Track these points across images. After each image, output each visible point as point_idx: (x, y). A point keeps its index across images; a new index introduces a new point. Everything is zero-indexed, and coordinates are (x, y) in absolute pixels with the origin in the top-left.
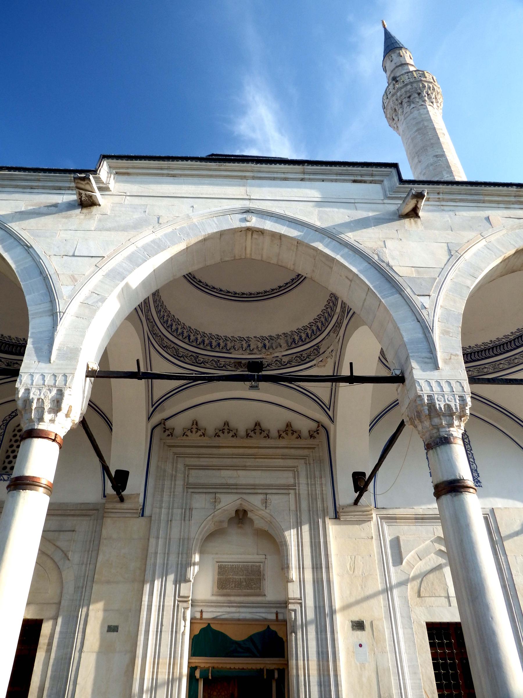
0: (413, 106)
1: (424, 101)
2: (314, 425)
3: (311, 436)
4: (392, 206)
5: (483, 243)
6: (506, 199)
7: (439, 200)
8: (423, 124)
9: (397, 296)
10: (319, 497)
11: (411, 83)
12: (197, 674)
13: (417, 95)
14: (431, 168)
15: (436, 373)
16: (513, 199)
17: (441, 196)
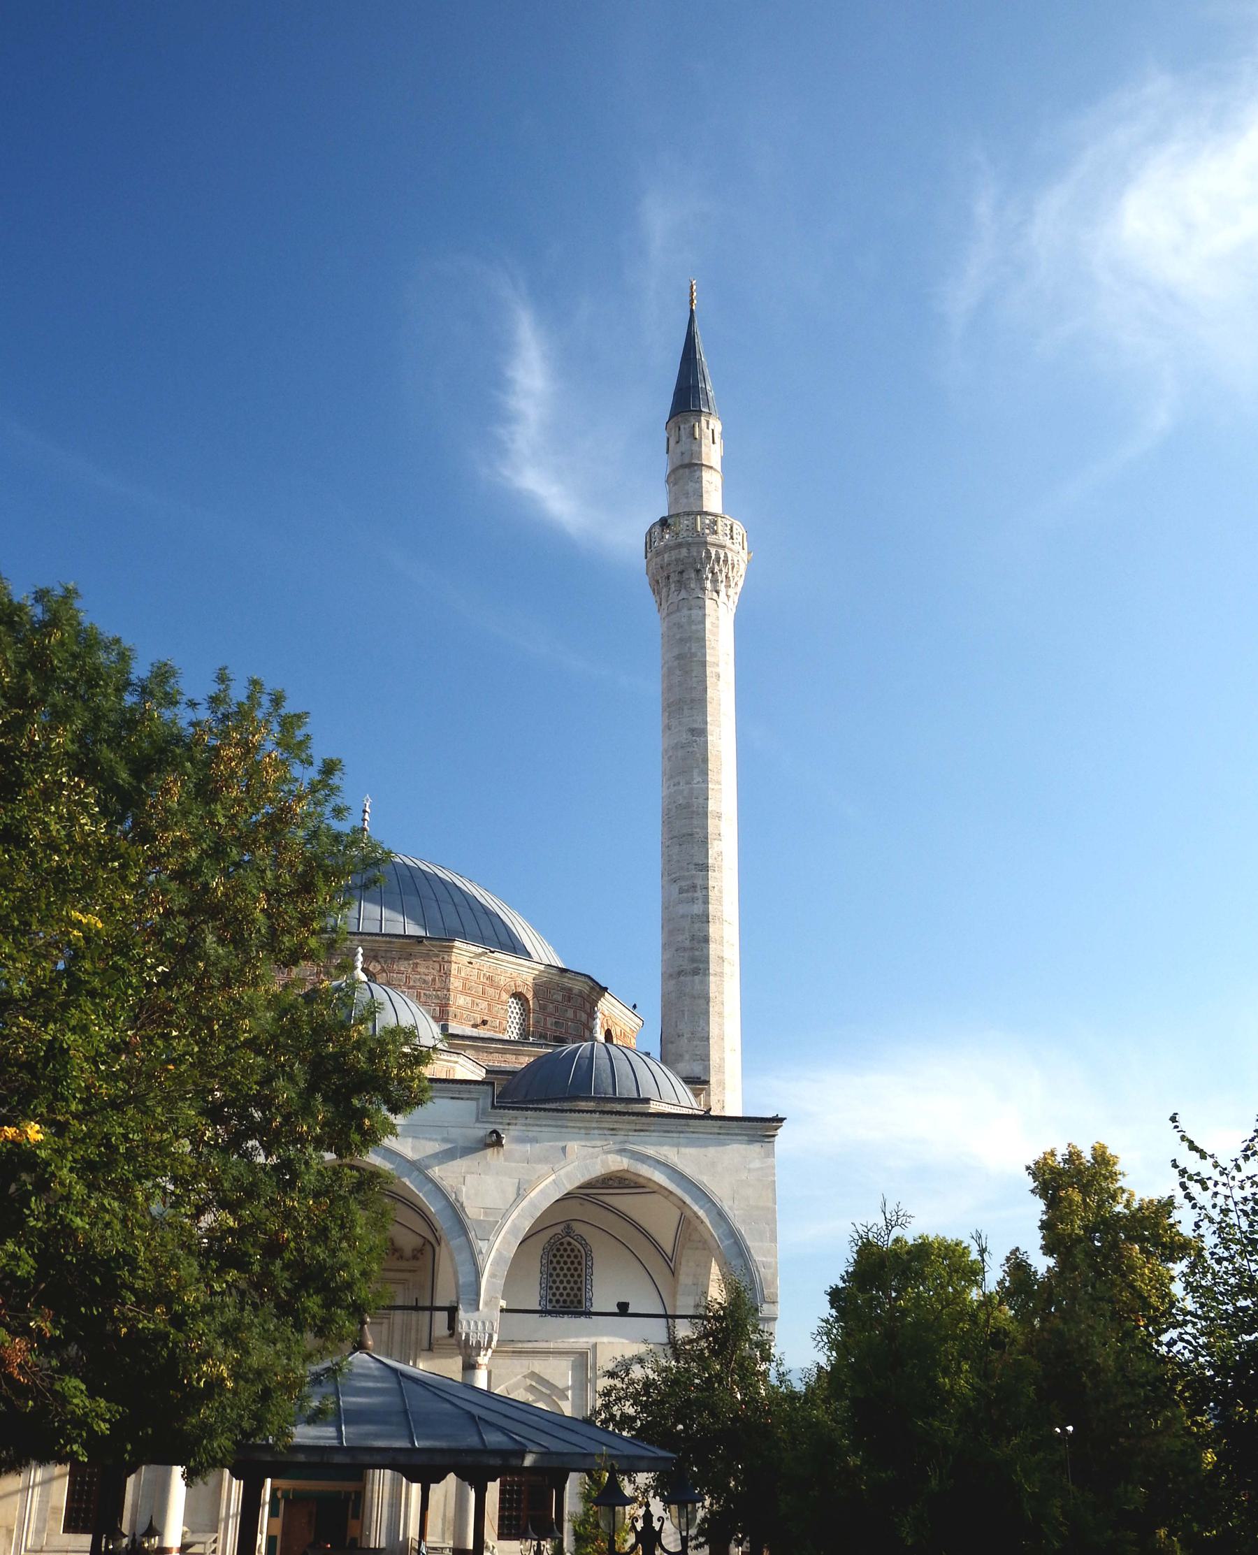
0: (683, 594)
1: (704, 589)
2: (420, 1241)
3: (415, 1258)
4: (481, 1131)
5: (553, 1177)
6: (587, 1125)
7: (526, 1125)
8: (690, 649)
9: (463, 1238)
10: (414, 1327)
11: (689, 545)
12: (279, 1495)
13: (693, 575)
14: (680, 753)
15: (477, 1314)
16: (594, 1125)
17: (528, 1121)
